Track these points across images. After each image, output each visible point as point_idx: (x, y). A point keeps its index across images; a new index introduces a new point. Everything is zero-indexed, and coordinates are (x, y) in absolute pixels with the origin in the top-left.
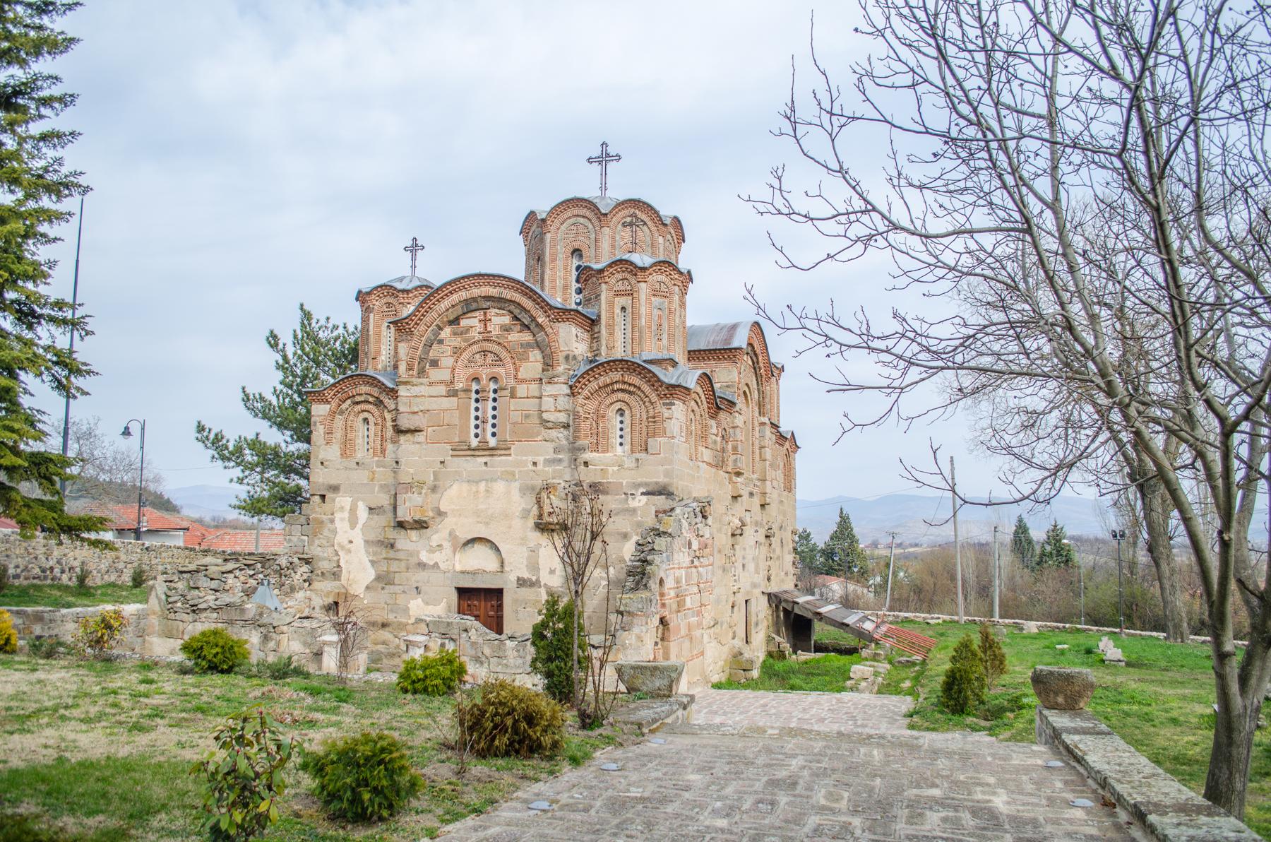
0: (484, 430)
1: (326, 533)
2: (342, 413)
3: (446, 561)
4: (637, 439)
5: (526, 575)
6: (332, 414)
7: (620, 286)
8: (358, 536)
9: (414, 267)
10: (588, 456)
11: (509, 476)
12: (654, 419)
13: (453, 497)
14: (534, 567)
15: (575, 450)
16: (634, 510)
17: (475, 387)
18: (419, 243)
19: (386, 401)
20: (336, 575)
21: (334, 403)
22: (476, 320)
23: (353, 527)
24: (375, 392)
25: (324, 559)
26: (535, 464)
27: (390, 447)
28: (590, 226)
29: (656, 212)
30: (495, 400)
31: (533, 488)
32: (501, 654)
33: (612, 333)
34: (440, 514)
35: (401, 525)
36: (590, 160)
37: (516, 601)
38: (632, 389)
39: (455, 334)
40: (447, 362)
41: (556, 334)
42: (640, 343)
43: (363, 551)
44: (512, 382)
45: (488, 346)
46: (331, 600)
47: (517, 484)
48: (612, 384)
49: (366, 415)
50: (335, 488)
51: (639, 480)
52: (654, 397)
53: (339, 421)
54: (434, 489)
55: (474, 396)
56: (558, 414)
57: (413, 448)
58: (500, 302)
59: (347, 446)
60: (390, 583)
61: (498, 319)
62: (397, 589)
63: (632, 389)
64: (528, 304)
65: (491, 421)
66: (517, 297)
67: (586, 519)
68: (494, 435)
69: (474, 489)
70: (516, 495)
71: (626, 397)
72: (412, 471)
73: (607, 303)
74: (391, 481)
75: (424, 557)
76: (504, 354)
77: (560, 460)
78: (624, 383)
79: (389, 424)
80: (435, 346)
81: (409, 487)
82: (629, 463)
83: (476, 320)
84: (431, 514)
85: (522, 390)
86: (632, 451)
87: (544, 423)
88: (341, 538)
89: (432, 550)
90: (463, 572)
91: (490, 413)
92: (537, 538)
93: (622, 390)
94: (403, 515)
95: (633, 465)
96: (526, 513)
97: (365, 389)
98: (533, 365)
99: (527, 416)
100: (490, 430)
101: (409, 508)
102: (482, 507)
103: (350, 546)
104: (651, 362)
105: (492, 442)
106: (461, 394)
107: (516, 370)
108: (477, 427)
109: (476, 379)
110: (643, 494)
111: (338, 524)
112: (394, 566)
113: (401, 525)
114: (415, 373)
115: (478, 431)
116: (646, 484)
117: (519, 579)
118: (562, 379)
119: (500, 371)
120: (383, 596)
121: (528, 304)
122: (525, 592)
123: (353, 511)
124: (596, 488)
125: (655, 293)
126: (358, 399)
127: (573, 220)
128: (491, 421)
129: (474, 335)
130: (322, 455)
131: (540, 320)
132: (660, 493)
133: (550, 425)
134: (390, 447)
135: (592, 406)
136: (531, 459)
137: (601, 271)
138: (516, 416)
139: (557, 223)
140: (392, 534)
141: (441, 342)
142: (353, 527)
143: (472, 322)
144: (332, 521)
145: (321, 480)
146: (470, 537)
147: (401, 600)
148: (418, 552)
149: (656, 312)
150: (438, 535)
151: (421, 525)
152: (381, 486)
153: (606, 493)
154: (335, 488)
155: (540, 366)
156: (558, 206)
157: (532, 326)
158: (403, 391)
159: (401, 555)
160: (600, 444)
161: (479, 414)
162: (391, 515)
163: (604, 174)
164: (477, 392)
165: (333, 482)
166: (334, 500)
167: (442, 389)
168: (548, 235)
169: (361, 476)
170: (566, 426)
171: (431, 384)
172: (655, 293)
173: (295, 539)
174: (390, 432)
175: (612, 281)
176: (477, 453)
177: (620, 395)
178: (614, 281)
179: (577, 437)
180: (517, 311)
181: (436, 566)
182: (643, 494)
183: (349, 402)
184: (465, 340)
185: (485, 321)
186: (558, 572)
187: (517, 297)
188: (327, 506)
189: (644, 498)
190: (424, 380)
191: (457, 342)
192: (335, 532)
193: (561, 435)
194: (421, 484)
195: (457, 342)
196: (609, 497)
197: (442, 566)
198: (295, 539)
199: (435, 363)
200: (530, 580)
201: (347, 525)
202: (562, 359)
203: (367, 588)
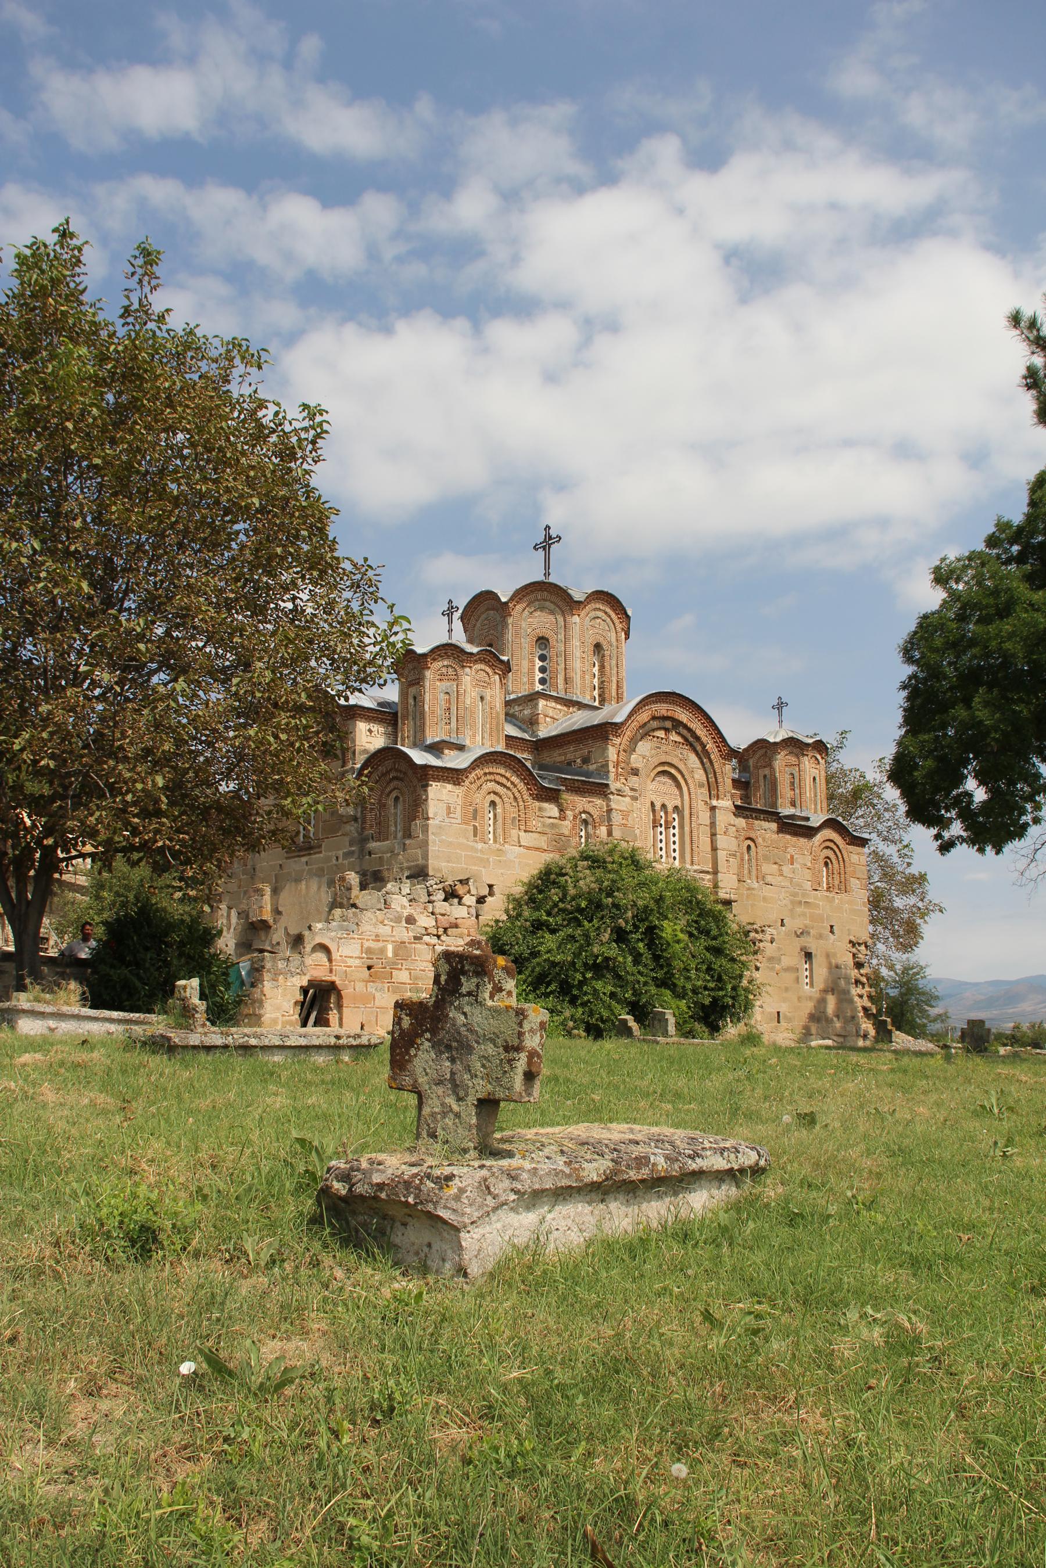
48: (388, 772)
52: (415, 781)
77: (353, 852)
116: (409, 868)
193: (352, 828)
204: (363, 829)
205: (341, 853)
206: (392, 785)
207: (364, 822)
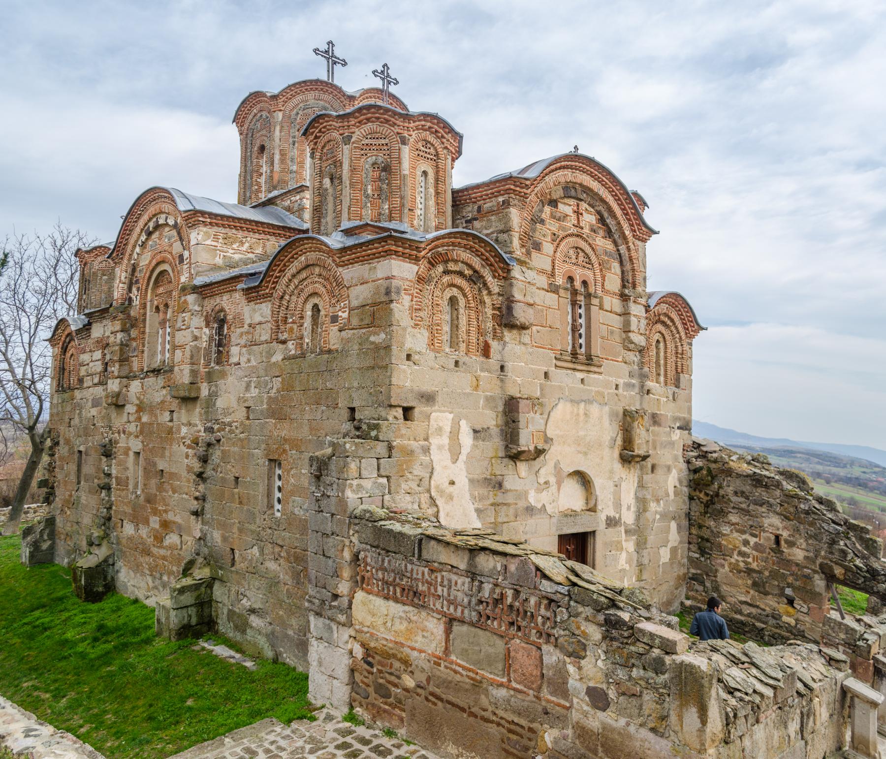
1: (418, 471)
8: (460, 473)
23: (455, 461)
26: (617, 386)
38: (669, 322)
47: (606, 409)
50: (429, 398)
57: (519, 349)
63: (669, 322)
72: (519, 380)
74: (497, 392)
75: (534, 499)
77: (634, 385)
86: (666, 384)
88: (440, 479)
89: (539, 491)
102: (581, 433)
103: (451, 489)
111: (435, 455)
123: (454, 435)
133: (632, 346)
134: (494, 345)
142: (455, 461)
144: (426, 450)
148: (526, 493)
150: (546, 469)
154: (429, 398)
165: (427, 388)
166: (428, 417)
173: (367, 484)
188: (417, 426)
193: (633, 357)
201: (447, 455)
205: (621, 382)
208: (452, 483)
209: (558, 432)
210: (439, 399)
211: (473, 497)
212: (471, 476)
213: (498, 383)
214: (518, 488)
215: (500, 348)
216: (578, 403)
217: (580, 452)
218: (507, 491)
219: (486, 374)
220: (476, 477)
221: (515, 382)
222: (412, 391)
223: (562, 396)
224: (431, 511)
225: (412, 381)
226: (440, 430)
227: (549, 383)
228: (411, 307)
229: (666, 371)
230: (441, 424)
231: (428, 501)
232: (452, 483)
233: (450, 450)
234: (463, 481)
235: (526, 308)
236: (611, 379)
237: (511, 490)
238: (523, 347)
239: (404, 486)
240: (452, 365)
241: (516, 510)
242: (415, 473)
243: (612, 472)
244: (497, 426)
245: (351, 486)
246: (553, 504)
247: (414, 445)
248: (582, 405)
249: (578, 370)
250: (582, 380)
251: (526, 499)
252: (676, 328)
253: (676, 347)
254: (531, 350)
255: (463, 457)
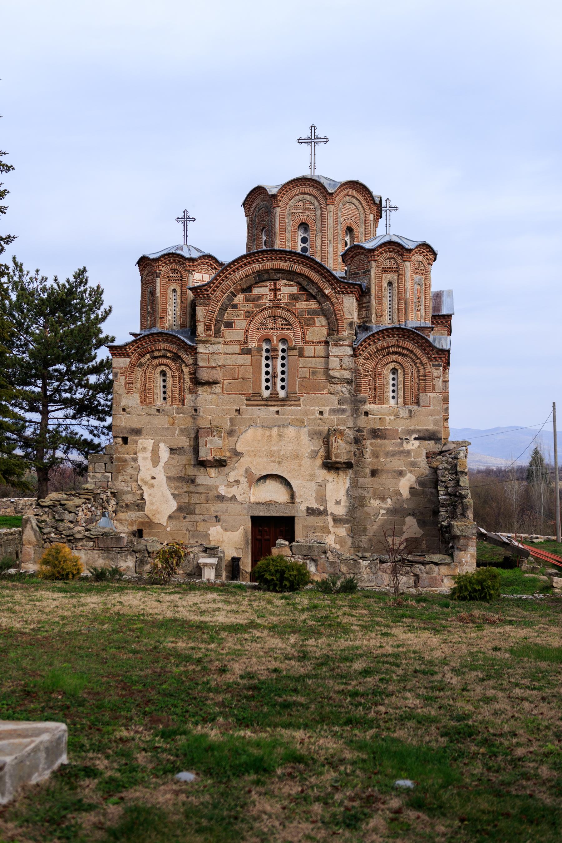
0: (274, 384)
1: (129, 470)
2: (141, 365)
3: (242, 494)
4: (408, 394)
5: (315, 505)
6: (132, 366)
7: (387, 264)
8: (160, 473)
9: (185, 236)
10: (368, 407)
11: (299, 423)
12: (425, 377)
13: (248, 440)
14: (322, 499)
15: (356, 402)
16: (408, 453)
17: (265, 346)
18: (181, 215)
19: (184, 356)
20: (140, 506)
21: (134, 357)
22: (267, 289)
24: (174, 348)
25: (127, 493)
26: (321, 413)
27: (188, 397)
28: (316, 204)
29: (370, 193)
30: (283, 358)
31: (320, 433)
32: (356, 571)
33: (380, 304)
34: (237, 454)
35: (202, 464)
36: (300, 141)
37: (306, 527)
38: (405, 352)
39: (247, 300)
40: (241, 324)
41: (341, 304)
42: (406, 313)
43: (165, 485)
44: (300, 344)
45: (279, 312)
46: (135, 528)
47: (306, 430)
48: (388, 347)
49: (163, 368)
50: (137, 432)
51: (413, 427)
52: (425, 360)
53: (139, 373)
54: (231, 433)
55: (264, 354)
56: (343, 372)
58: (289, 275)
59: (146, 396)
60: (192, 513)
61: (287, 289)
62: (198, 518)
63: (405, 352)
64: (315, 277)
65: (280, 376)
66: (306, 271)
67: (368, 458)
68: (283, 387)
69: (267, 433)
70: (305, 439)
71: (400, 358)
72: (210, 417)
73: (377, 278)
74: (190, 425)
75: (222, 490)
76: (292, 319)
77: (344, 411)
78: (399, 347)
79: (187, 377)
80: (229, 310)
81: (211, 431)
82: (403, 413)
83: (267, 289)
84: (228, 454)
85: (309, 350)
86: (405, 403)
87: (330, 379)
89: (229, 485)
90: (258, 503)
91: (279, 369)
92: (323, 474)
93: (397, 353)
94: (204, 454)
95: (407, 415)
96: (314, 455)
97: (163, 345)
98: (319, 329)
99: (314, 373)
100: (279, 384)
101: (210, 448)
102: (275, 448)
103: (153, 481)
104: (415, 328)
105: (282, 394)
106: (254, 353)
107: (304, 333)
108: (267, 380)
109: (268, 340)
110: (415, 439)
111: (141, 462)
112: (195, 499)
113: (202, 464)
114: (212, 333)
115: (269, 384)
116: (418, 431)
117: (308, 509)
118: (347, 342)
119: (290, 334)
120: (185, 524)
121: (315, 277)
122: (313, 520)
124: (376, 434)
125: (416, 271)
126: (157, 354)
127: (300, 197)
128: (280, 376)
129: (266, 302)
130: (124, 402)
131: (327, 292)
132: (430, 439)
134: (188, 397)
135: (370, 365)
136: (317, 408)
137: (372, 250)
138: (305, 373)
139: (285, 199)
140: (192, 471)
141: (235, 307)
143: (263, 290)
144: (135, 460)
145: (123, 424)
146: (264, 474)
147: (201, 527)
148: (217, 487)
149: (416, 287)
150: (236, 472)
151: (220, 464)
152: (181, 430)
153: (383, 437)
154: (137, 432)
155: (325, 331)
156: (288, 184)
157: (319, 297)
158: (201, 349)
159: (201, 489)
160: (378, 397)
161: (270, 369)
162: (190, 455)
163: (313, 155)
164: (267, 351)
165: (136, 426)
166: (136, 442)
167: (237, 348)
168: (278, 209)
169: (163, 421)
170: (349, 382)
171: (226, 343)
172: (416, 271)
173: (99, 476)
174: (188, 384)
175: (380, 259)
176: (270, 403)
177: (394, 357)
178: (383, 260)
179: (358, 393)
180: (305, 283)
181: (234, 498)
182: (415, 439)
183: (148, 356)
184: (257, 306)
185: (275, 290)
186: (343, 503)
187: (306, 271)
188: (129, 447)
189: (417, 443)
190: (221, 340)
191: (249, 307)
192: (138, 470)
193: (344, 389)
194: (219, 429)
195: (249, 307)
196: (386, 442)
197: (239, 498)
198: (99, 476)
199: (229, 325)
200: (318, 509)
201: (149, 463)
202: (346, 325)
203: (170, 517)
204: (356, 391)
205: (326, 409)
206: (390, 358)
207: (358, 385)
208: (154, 478)
209: (248, 448)
210: (144, 431)
211: (170, 487)
212: (168, 475)
213: (192, 420)
214: (209, 484)
215: (194, 398)
216: (270, 428)
217: (272, 461)
218: (198, 485)
219: (181, 415)
220: (172, 475)
221: (206, 419)
222: (126, 428)
223: (252, 423)
224: (139, 492)
225: (126, 423)
226: (144, 449)
227: (240, 416)
228: (125, 383)
229: (404, 393)
230: (145, 446)
231: (137, 487)
232: (154, 478)
233: (152, 460)
234: (161, 477)
235: (209, 370)
236: (312, 408)
237: (202, 485)
238: (214, 396)
239: (120, 478)
240: (155, 412)
241: (207, 497)
242: (128, 471)
243: (312, 476)
244: (190, 446)
245: (90, 476)
246: (243, 496)
247: (127, 457)
248: (275, 430)
249: (271, 405)
250: (277, 412)
251: (217, 490)
252: (415, 355)
253: (418, 371)
254: (221, 397)
255: (162, 464)
